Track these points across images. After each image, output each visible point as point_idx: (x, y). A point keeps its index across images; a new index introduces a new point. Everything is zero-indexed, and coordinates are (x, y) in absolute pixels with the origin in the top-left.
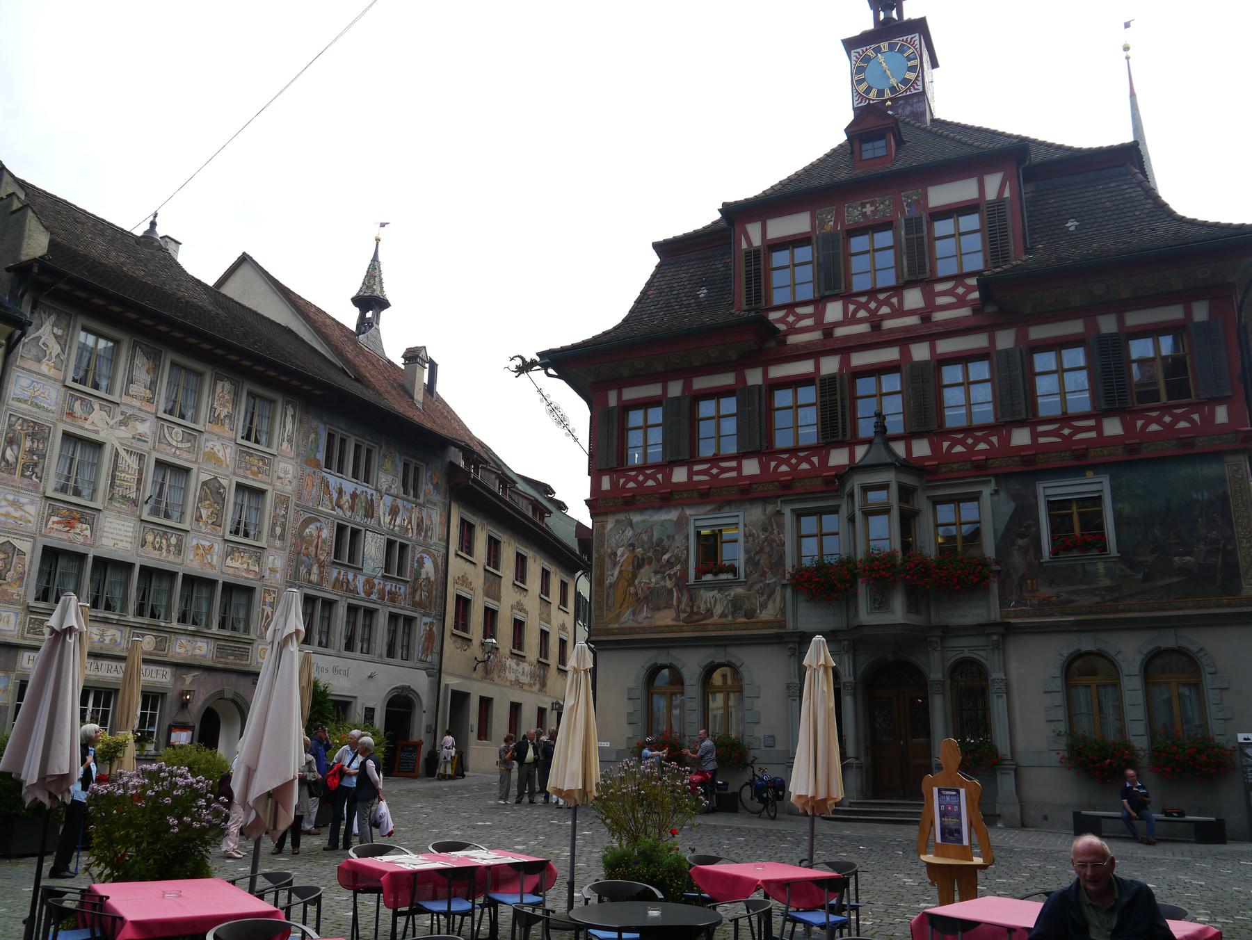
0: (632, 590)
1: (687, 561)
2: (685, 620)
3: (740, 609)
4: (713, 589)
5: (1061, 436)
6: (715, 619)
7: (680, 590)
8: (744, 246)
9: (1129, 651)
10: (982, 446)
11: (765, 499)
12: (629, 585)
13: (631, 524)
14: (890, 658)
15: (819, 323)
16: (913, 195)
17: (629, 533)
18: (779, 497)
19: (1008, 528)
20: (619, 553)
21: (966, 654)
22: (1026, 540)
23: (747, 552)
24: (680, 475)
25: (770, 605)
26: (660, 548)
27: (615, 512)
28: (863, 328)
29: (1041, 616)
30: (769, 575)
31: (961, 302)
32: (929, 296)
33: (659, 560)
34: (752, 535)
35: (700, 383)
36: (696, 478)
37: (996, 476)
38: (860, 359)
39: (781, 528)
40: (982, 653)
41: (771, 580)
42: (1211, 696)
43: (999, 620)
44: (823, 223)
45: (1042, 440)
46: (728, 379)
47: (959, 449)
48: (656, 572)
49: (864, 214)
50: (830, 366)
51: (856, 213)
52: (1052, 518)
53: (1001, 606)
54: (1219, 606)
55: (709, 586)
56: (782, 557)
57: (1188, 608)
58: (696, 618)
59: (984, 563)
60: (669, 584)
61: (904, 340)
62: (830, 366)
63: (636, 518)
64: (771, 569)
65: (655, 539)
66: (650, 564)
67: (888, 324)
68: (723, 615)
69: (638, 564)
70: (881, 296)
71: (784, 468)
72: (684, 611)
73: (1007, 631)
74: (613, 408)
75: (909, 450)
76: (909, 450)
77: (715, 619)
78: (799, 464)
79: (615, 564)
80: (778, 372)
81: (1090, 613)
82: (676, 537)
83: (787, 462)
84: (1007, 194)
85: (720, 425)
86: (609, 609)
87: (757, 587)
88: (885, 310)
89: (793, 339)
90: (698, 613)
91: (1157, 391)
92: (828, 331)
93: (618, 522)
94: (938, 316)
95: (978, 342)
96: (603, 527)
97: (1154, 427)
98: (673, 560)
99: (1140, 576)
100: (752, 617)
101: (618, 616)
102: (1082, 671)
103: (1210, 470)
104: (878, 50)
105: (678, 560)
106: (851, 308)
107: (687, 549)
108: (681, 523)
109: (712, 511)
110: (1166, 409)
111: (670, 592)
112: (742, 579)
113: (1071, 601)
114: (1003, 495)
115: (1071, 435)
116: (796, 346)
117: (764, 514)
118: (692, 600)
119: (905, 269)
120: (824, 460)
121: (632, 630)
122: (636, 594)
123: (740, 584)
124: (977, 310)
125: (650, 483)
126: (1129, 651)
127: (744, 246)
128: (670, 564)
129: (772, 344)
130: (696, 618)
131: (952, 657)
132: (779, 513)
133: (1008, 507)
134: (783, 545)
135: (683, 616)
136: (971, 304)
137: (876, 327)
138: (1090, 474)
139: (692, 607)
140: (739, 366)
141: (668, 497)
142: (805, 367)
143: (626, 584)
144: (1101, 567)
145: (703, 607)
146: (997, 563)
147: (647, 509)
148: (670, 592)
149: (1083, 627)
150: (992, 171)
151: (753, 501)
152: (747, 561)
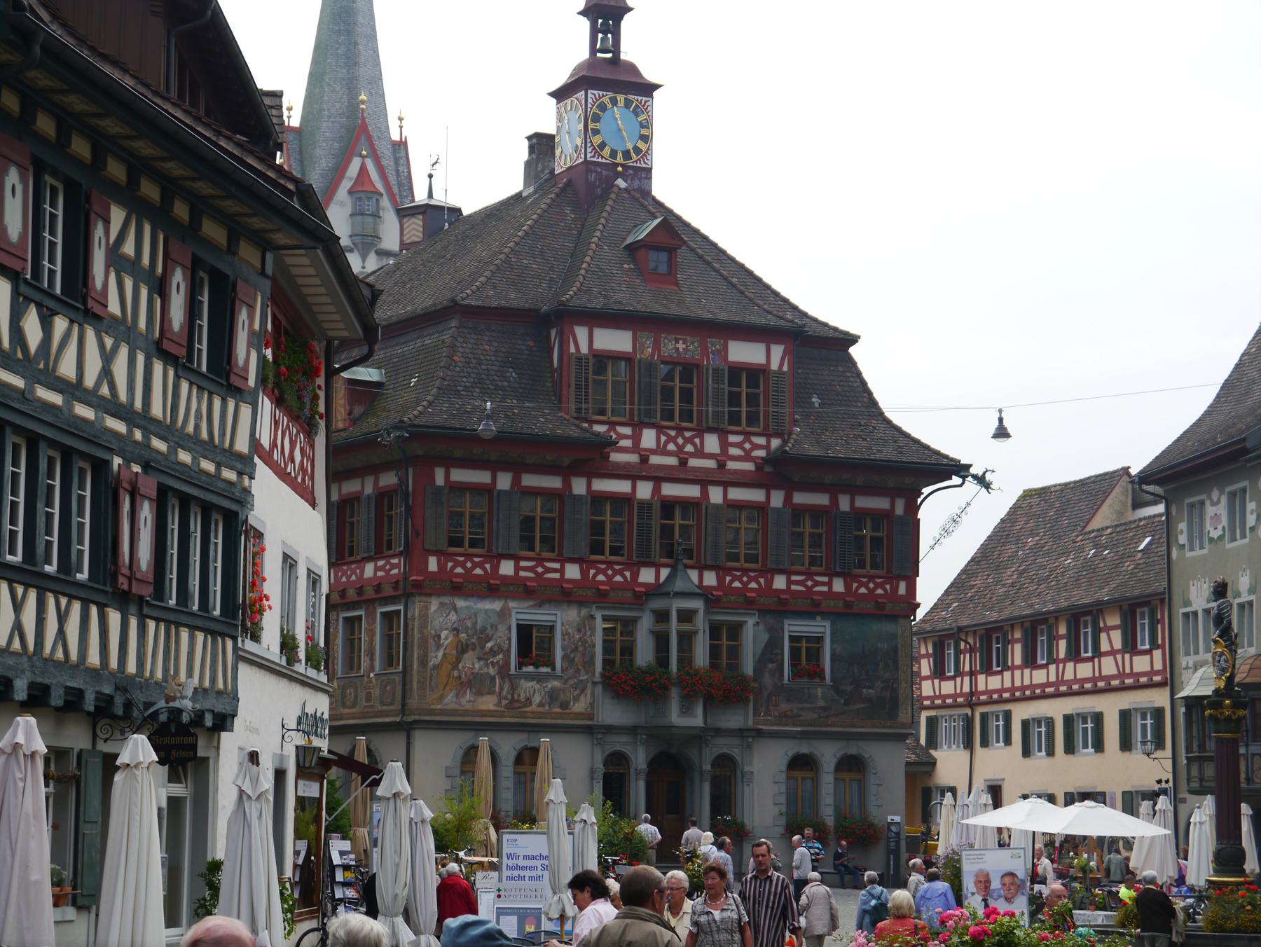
0: (456, 673)
1: (509, 651)
2: (506, 706)
4: (533, 680)
5: (806, 586)
6: (534, 707)
7: (502, 678)
8: (572, 350)
9: (828, 754)
11: (581, 603)
13: (455, 608)
16: (714, 344)
17: (453, 617)
19: (763, 653)
21: (725, 751)
23: (563, 649)
25: (582, 698)
26: (484, 636)
28: (672, 461)
29: (780, 725)
30: (582, 672)
31: (747, 457)
32: (724, 445)
33: (483, 647)
34: (568, 634)
36: (522, 574)
38: (669, 490)
39: (593, 630)
40: (736, 751)
42: (872, 789)
45: (794, 587)
48: (479, 659)
50: (644, 491)
51: (671, 346)
52: (791, 648)
55: (529, 677)
56: (593, 657)
58: (517, 705)
60: (492, 671)
61: (704, 480)
63: (460, 603)
65: (479, 626)
66: (474, 650)
67: (693, 462)
68: (541, 705)
69: (463, 649)
70: (688, 434)
71: (601, 578)
72: (505, 698)
73: (759, 734)
77: (534, 707)
78: (613, 575)
79: (439, 646)
81: (810, 725)
84: (785, 368)
86: (432, 689)
87: (571, 682)
88: (689, 448)
89: (616, 457)
90: (518, 701)
93: (441, 604)
94: (731, 465)
95: (756, 495)
96: (427, 608)
97: (863, 590)
101: (441, 698)
102: (801, 764)
103: (889, 627)
104: (614, 102)
105: (501, 649)
106: (663, 438)
107: (509, 639)
108: (504, 614)
111: (493, 678)
116: (617, 465)
118: (513, 688)
120: (635, 575)
122: (460, 677)
124: (759, 468)
125: (478, 571)
126: (828, 754)
127: (572, 350)
128: (493, 652)
130: (517, 705)
131: (717, 751)
132: (592, 617)
133: (765, 637)
135: (504, 702)
137: (683, 463)
140: (567, 473)
142: (623, 487)
144: (819, 691)
145: (523, 696)
146: (754, 681)
147: (472, 596)
148: (493, 678)
149: (804, 736)
150: (778, 342)
152: (565, 657)
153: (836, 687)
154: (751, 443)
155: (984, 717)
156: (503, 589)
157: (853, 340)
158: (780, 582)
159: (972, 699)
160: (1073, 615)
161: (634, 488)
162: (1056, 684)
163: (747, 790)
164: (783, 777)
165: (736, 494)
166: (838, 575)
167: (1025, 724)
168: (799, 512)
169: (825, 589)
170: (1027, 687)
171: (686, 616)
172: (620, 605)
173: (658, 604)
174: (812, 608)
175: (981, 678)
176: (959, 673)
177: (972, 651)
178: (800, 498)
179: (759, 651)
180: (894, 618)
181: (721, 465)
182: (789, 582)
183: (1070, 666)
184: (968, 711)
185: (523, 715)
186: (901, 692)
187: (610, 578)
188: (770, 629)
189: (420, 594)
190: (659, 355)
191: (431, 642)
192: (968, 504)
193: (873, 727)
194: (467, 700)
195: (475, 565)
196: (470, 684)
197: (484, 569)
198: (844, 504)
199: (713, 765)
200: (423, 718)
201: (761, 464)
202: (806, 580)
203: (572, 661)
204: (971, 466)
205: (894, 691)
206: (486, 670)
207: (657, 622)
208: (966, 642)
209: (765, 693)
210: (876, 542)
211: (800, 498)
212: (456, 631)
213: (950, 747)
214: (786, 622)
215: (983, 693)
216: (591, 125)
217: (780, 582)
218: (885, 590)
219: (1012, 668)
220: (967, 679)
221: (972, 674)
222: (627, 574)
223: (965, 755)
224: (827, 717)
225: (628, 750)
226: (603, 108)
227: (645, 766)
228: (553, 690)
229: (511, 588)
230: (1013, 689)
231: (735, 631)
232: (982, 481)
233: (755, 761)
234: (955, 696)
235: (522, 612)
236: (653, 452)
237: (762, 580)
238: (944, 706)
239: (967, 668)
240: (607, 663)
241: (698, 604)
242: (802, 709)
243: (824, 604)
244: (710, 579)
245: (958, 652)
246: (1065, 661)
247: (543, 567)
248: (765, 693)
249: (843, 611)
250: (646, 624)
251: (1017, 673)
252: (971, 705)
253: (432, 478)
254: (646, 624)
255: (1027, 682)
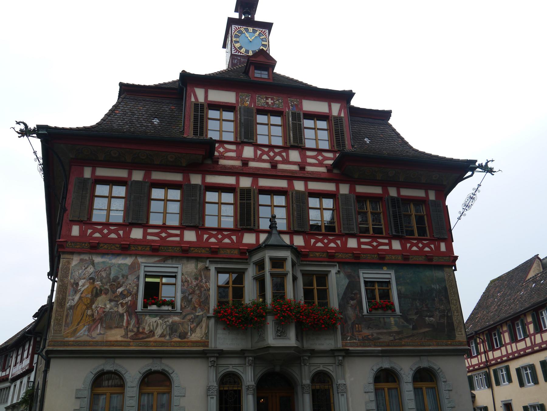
0: (89, 312)
1: (137, 294)
2: (132, 338)
3: (176, 331)
4: (156, 316)
5: (373, 246)
6: (156, 338)
7: (129, 315)
8: (193, 99)
9: (406, 368)
10: (332, 245)
11: (198, 259)
12: (87, 308)
13: (93, 264)
14: (278, 369)
15: (239, 157)
16: (292, 101)
17: (91, 269)
18: (208, 258)
19: (345, 293)
20: (80, 283)
21: (321, 368)
22: (355, 301)
23: (183, 292)
24: (137, 234)
25: (198, 329)
27: (80, 253)
28: (267, 165)
30: (198, 309)
31: (320, 164)
32: (304, 157)
33: (114, 292)
34: (187, 281)
35: (157, 176)
36: (149, 237)
37: (339, 263)
38: (264, 183)
39: (208, 278)
40: (331, 368)
41: (199, 313)
43: (341, 348)
44: (243, 101)
45: (363, 247)
46: (177, 177)
47: (320, 244)
48: (111, 301)
49: (267, 103)
50: (246, 182)
53: (343, 339)
54: (447, 345)
55: (153, 314)
56: (207, 298)
57: (434, 345)
58: (141, 336)
59: (332, 311)
60: (121, 310)
61: (290, 177)
62: (246, 182)
64: (200, 306)
65: (112, 276)
66: (106, 294)
67: (281, 166)
69: (97, 293)
70: (277, 150)
71: (213, 240)
72: (132, 331)
73: (347, 354)
74: (89, 179)
75: (292, 240)
76: (292, 240)
77: (156, 338)
79: (76, 292)
80: (212, 179)
81: (388, 346)
82: (130, 277)
83: (215, 236)
85: (166, 207)
86: (67, 325)
87: (189, 317)
88: (278, 158)
89: (222, 162)
90: (143, 333)
91: (413, 231)
92: (245, 162)
94: (309, 169)
95: (330, 187)
96: (69, 263)
97: (415, 248)
98: (126, 293)
99: (411, 327)
100: (185, 338)
101: (75, 331)
102: (386, 378)
103: (438, 274)
105: (130, 293)
106: (259, 152)
107: (138, 286)
108: (134, 268)
109: (159, 262)
110: (420, 240)
111: (122, 316)
112: (179, 310)
113: (379, 339)
114: (342, 274)
115: (377, 246)
116: (224, 166)
117: (196, 269)
118: (139, 323)
119: (292, 139)
120: (240, 239)
121: (86, 343)
122: (93, 315)
123: (176, 314)
125: (113, 236)
126: (406, 368)
127: (193, 99)
128: (123, 295)
129: (209, 162)
130: (141, 336)
131: (314, 369)
132: (207, 269)
133: (345, 282)
134: (209, 290)
135: (130, 334)
136: (326, 166)
137: (274, 166)
138: (385, 268)
139: (138, 328)
141: (126, 248)
142: (230, 180)
143: (84, 307)
145: (147, 329)
146: (341, 313)
147: (108, 254)
148: (122, 316)
149: (384, 354)
151: (189, 258)
153: (404, 315)
154: (323, 156)
155: (495, 372)
156: (133, 248)
157: (387, 114)
158: (352, 243)
159: (488, 365)
160: (534, 310)
161: (238, 181)
162: (532, 347)
163: (342, 400)
164: (371, 388)
165: (314, 186)
166: (395, 237)
167: (518, 370)
168: (362, 198)
169: (387, 247)
170: (515, 352)
171: (278, 263)
172: (230, 260)
173: (256, 258)
174: (380, 261)
175: (490, 354)
176: (479, 353)
177: (483, 342)
178: (360, 189)
179: (342, 292)
180: (440, 267)
181: (302, 168)
182: (359, 243)
183: (538, 336)
184: (487, 370)
185: (147, 344)
186: (454, 319)
187: (220, 241)
188: (349, 276)
189: (64, 253)
190: (255, 105)
191: (70, 289)
192: (479, 185)
193: (438, 345)
194: (98, 334)
195: (110, 232)
196: (101, 320)
197: (118, 235)
198: (393, 192)
199: (313, 381)
200: (55, 348)
201: (330, 169)
202: (372, 242)
203: (190, 301)
204: (476, 161)
205: (450, 318)
206: (116, 309)
207: (259, 271)
208: (480, 338)
209: (350, 323)
210: (420, 220)
211: (360, 189)
212: (92, 280)
213: (480, 388)
214: (361, 272)
215: (492, 360)
216: (234, 39)
217: (352, 243)
218: (430, 248)
219: (505, 345)
220: (483, 356)
221: (485, 352)
222: (234, 238)
223: (489, 391)
224: (400, 339)
225: (239, 370)
226: (241, 32)
227: (253, 383)
228: (173, 323)
229: (140, 248)
230: (508, 355)
231: (323, 278)
232: (487, 169)
233: (348, 375)
234: (479, 364)
235: (147, 264)
236: (253, 160)
237: (339, 242)
238: (475, 370)
239: (482, 350)
240: (220, 303)
241: (286, 254)
242: (381, 334)
243: (387, 257)
244: (299, 241)
245: (477, 344)
246: (534, 335)
247: (166, 233)
248: (350, 323)
249: (402, 263)
250: (251, 272)
251: (509, 347)
252: (488, 367)
253: (82, 173)
254: (251, 272)
255: (514, 350)
